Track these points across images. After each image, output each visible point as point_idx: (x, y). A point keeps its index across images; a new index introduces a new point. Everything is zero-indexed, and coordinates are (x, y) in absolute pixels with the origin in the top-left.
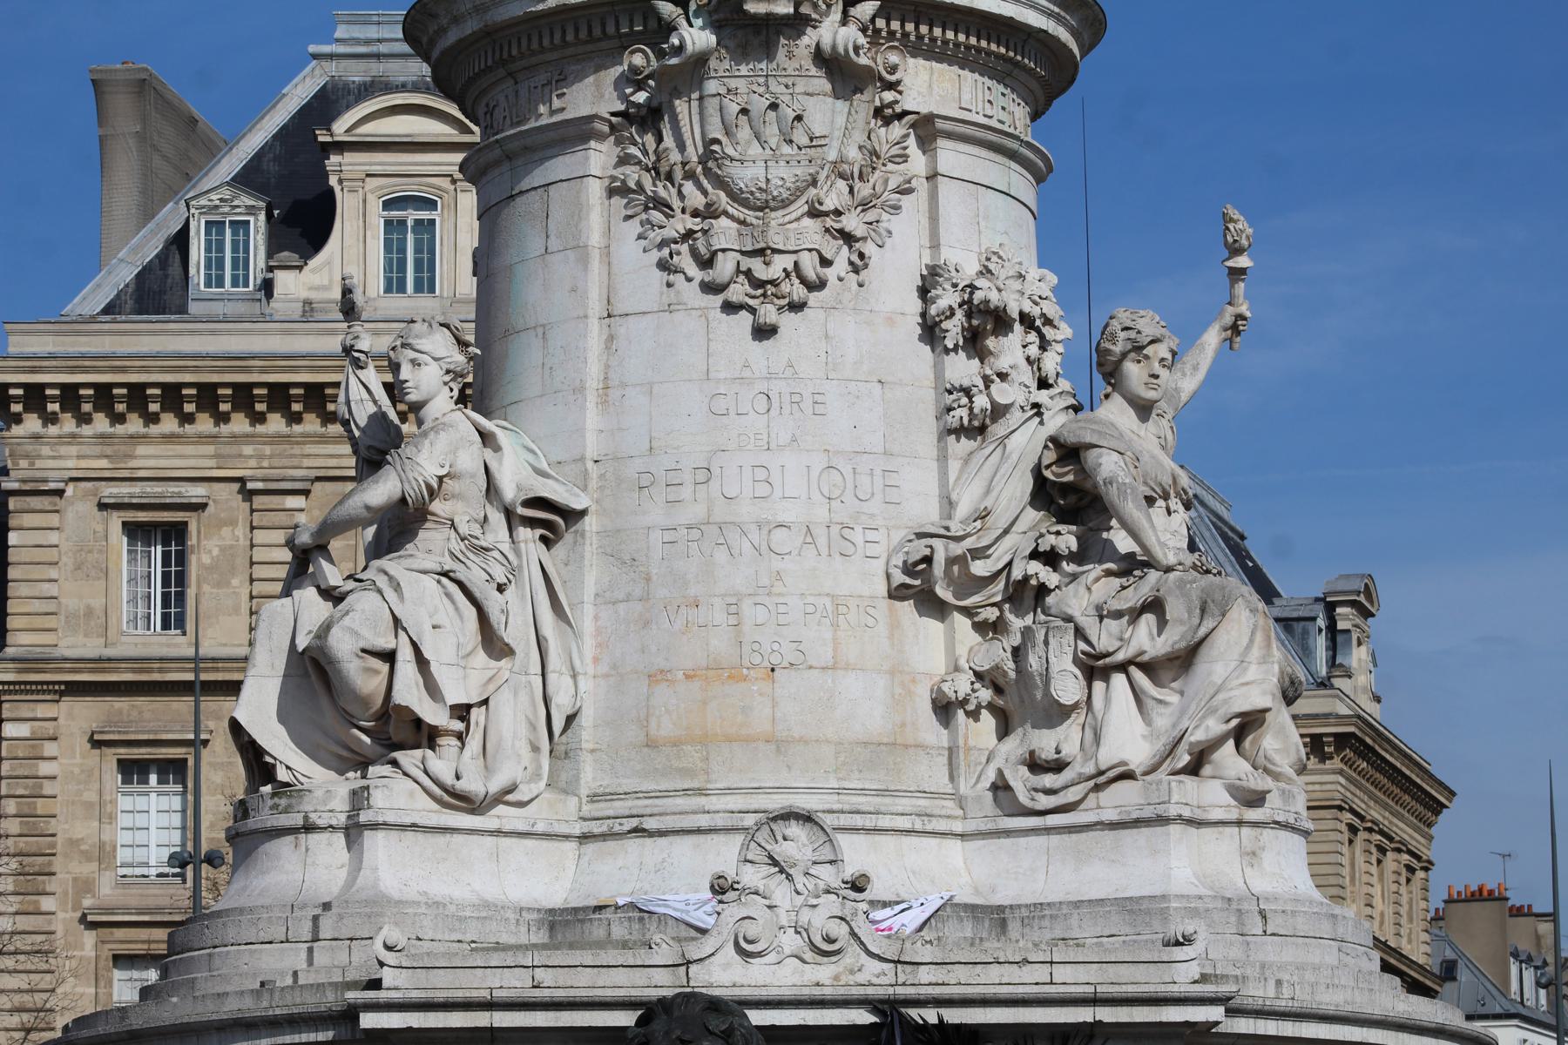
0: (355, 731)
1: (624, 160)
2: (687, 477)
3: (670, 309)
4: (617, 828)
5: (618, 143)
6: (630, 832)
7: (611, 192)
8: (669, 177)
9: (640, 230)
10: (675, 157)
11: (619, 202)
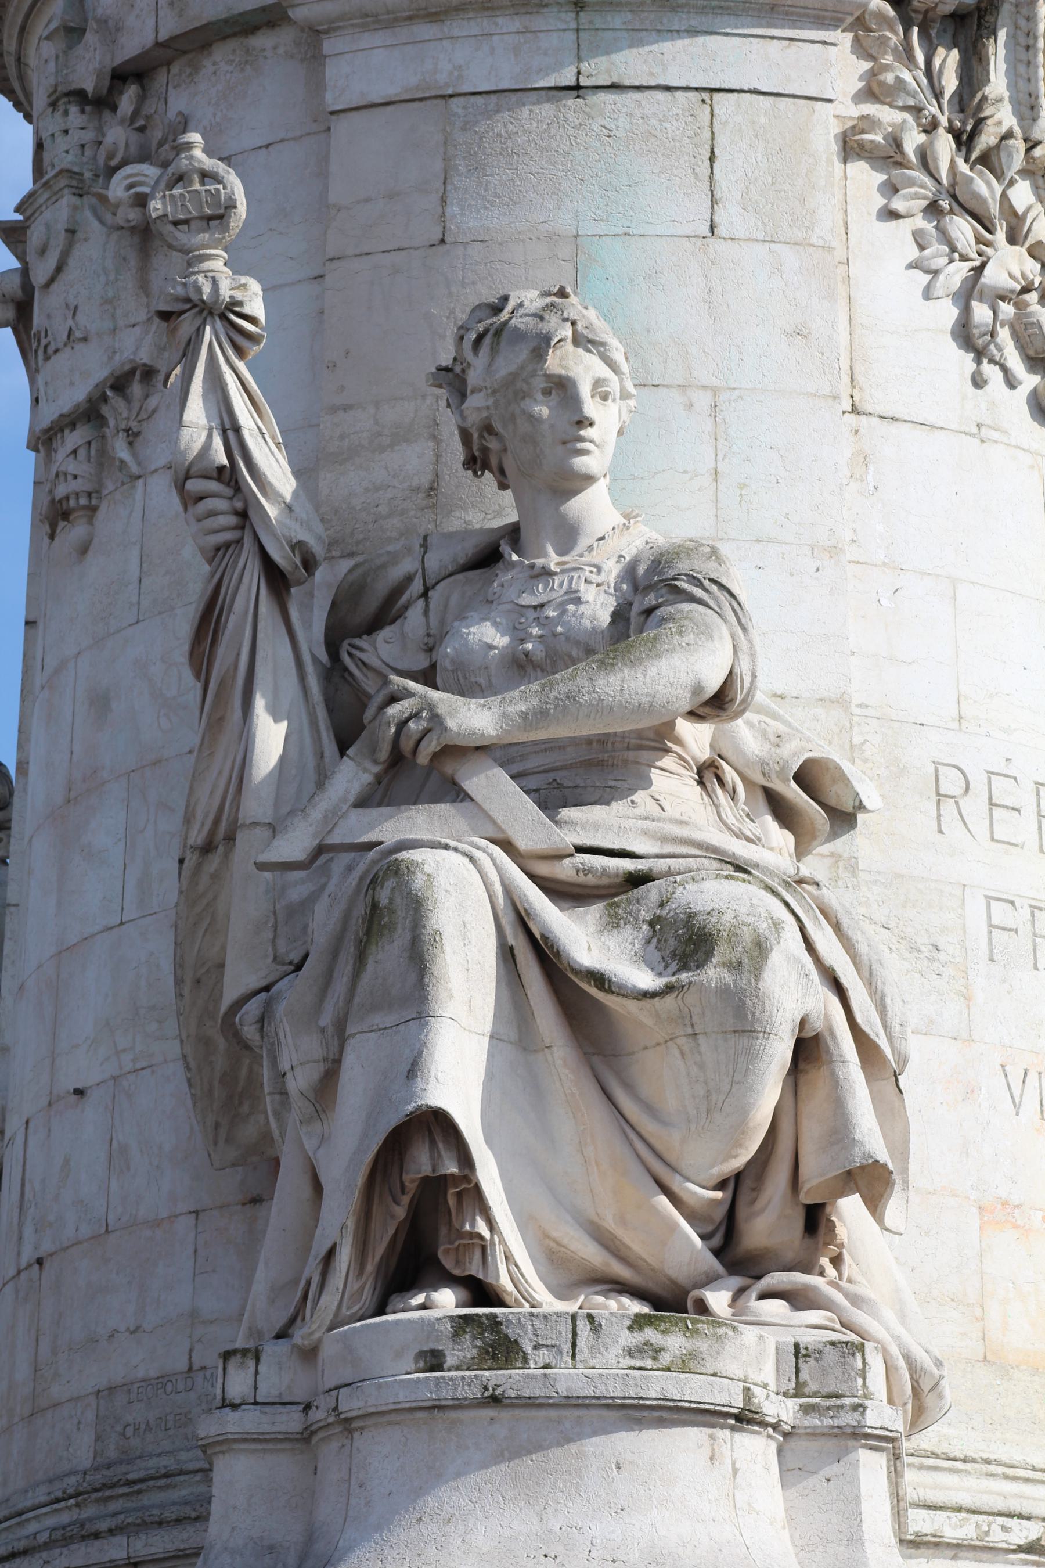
0: (663, 1199)
1: (873, 91)
2: (1026, 799)
3: (980, 431)
4: (997, 1537)
5: (860, 49)
6: (1020, 1549)
7: (851, 147)
8: (987, 160)
9: (913, 253)
10: (1002, 117)
11: (866, 178)
